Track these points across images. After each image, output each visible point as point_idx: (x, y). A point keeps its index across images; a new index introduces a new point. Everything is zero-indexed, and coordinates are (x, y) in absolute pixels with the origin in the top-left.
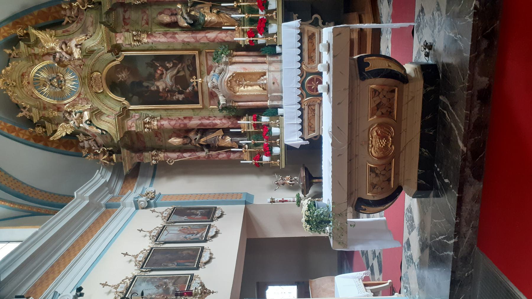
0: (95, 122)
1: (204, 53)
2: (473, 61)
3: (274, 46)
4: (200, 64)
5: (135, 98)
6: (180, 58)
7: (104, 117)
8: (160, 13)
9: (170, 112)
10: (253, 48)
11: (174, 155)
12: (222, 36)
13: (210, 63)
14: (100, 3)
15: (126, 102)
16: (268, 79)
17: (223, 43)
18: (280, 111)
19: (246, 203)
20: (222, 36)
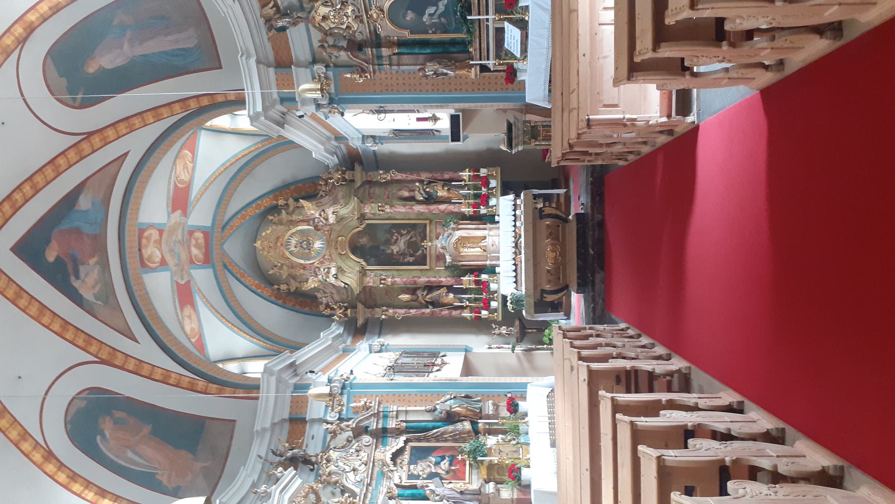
0: (340, 276)
1: (434, 222)
2: (592, 207)
4: (430, 231)
5: (372, 260)
7: (345, 274)
9: (401, 273)
11: (402, 311)
12: (451, 208)
13: (438, 231)
14: (353, 181)
15: (364, 263)
16: (489, 241)
17: (452, 213)
18: (497, 270)
19: (466, 351)
20: (451, 208)
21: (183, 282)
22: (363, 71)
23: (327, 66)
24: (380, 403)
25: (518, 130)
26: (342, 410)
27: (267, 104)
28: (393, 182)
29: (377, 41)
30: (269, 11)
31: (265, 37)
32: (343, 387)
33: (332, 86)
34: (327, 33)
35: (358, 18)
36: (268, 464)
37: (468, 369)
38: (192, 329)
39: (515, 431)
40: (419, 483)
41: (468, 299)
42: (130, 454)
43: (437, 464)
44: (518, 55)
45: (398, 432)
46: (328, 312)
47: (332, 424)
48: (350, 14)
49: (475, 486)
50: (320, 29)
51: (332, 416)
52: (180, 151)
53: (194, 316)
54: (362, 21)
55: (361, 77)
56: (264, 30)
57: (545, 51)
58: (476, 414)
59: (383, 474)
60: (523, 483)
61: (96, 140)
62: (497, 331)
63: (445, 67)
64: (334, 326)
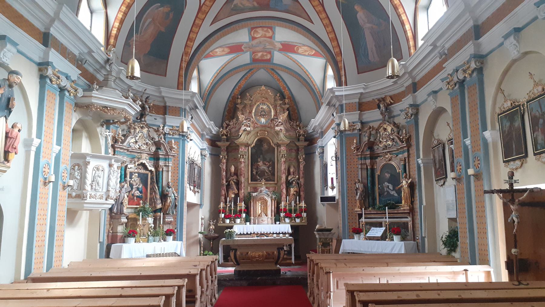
0: (245, 132)
2: (284, 279)
3: (279, 221)
5: (254, 151)
6: (273, 174)
7: (247, 135)
8: (294, 167)
10: (278, 211)
11: (224, 167)
12: (284, 196)
13: (271, 188)
16: (264, 218)
17: (281, 197)
18: (248, 223)
20: (284, 196)
21: (243, 48)
22: (358, 149)
23: (360, 130)
24: (173, 156)
25: (328, 235)
26: (170, 135)
27: (340, 98)
28: (299, 163)
29: (374, 157)
30: (388, 100)
31: (375, 98)
32: (183, 136)
33: (349, 132)
34: (377, 130)
35: (386, 147)
36: (141, 94)
37: (191, 206)
38: (216, 52)
39: (155, 234)
40: (128, 178)
41: (231, 206)
42: (149, 20)
43: (138, 189)
44: (367, 235)
45: (156, 166)
46: (225, 125)
47: (163, 129)
48: (388, 143)
49: (125, 211)
50: (380, 127)
51: (167, 129)
52: (314, 49)
53: (224, 53)
54: (384, 149)
55: (354, 148)
56: (379, 97)
57: (370, 250)
58: (166, 211)
59: (133, 158)
60: (126, 239)
61: (320, 8)
62: (212, 223)
63: (361, 195)
64: (216, 129)
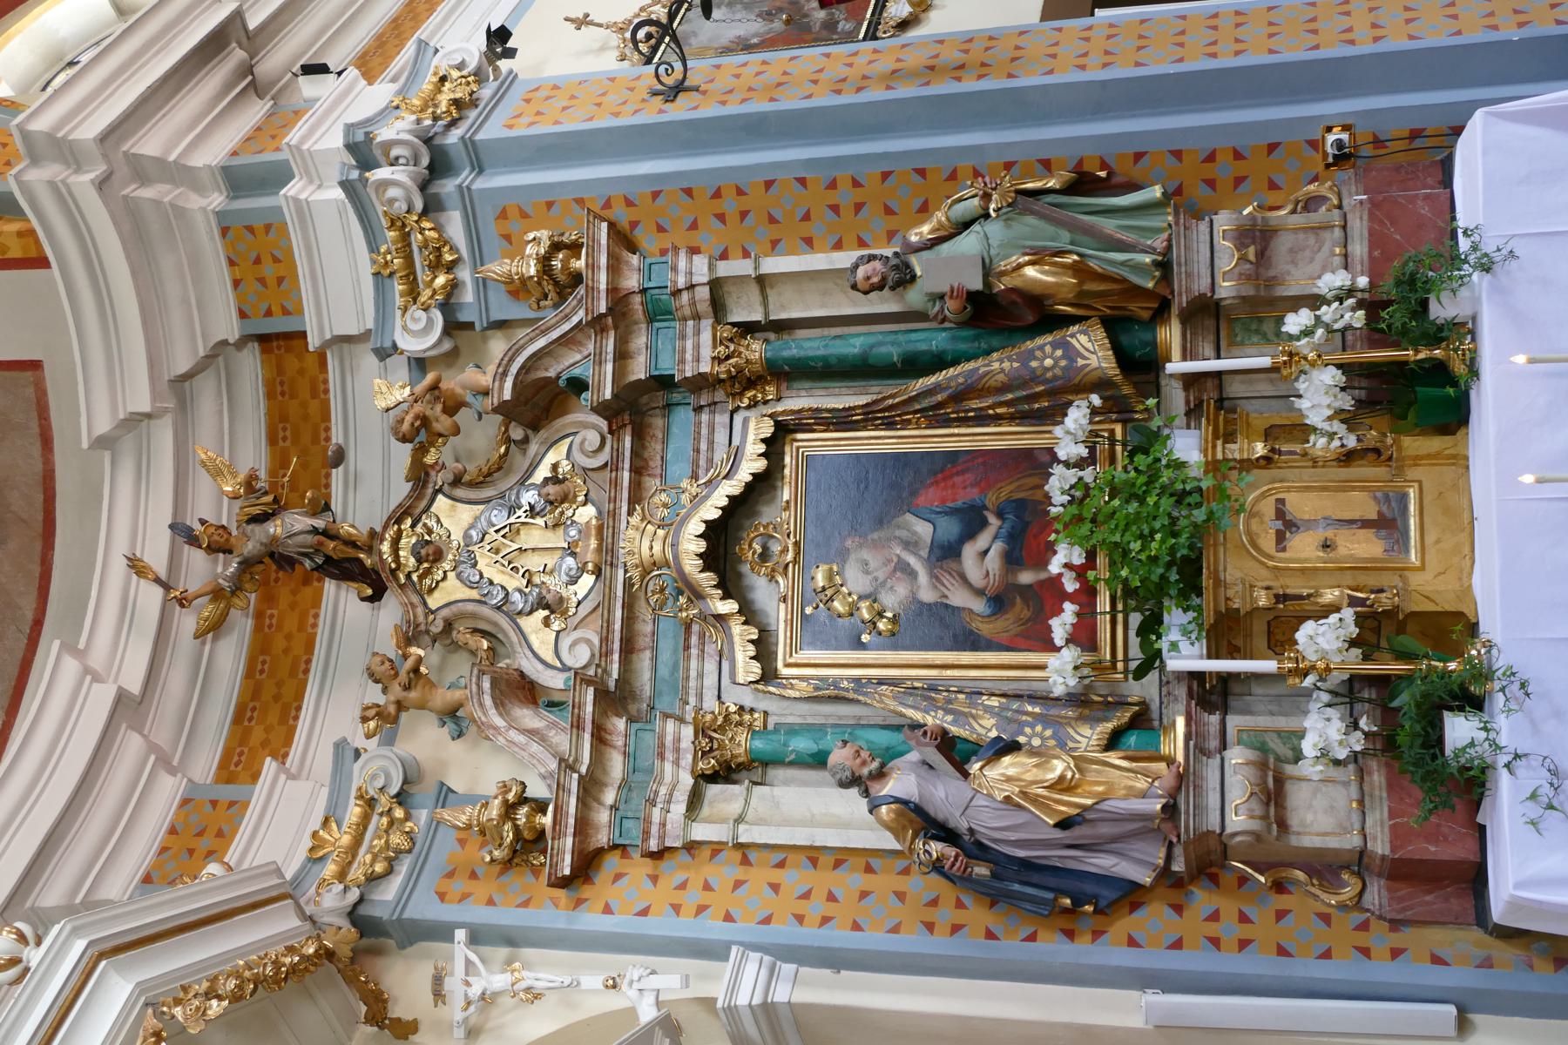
26: (454, 286)
43: (946, 554)
